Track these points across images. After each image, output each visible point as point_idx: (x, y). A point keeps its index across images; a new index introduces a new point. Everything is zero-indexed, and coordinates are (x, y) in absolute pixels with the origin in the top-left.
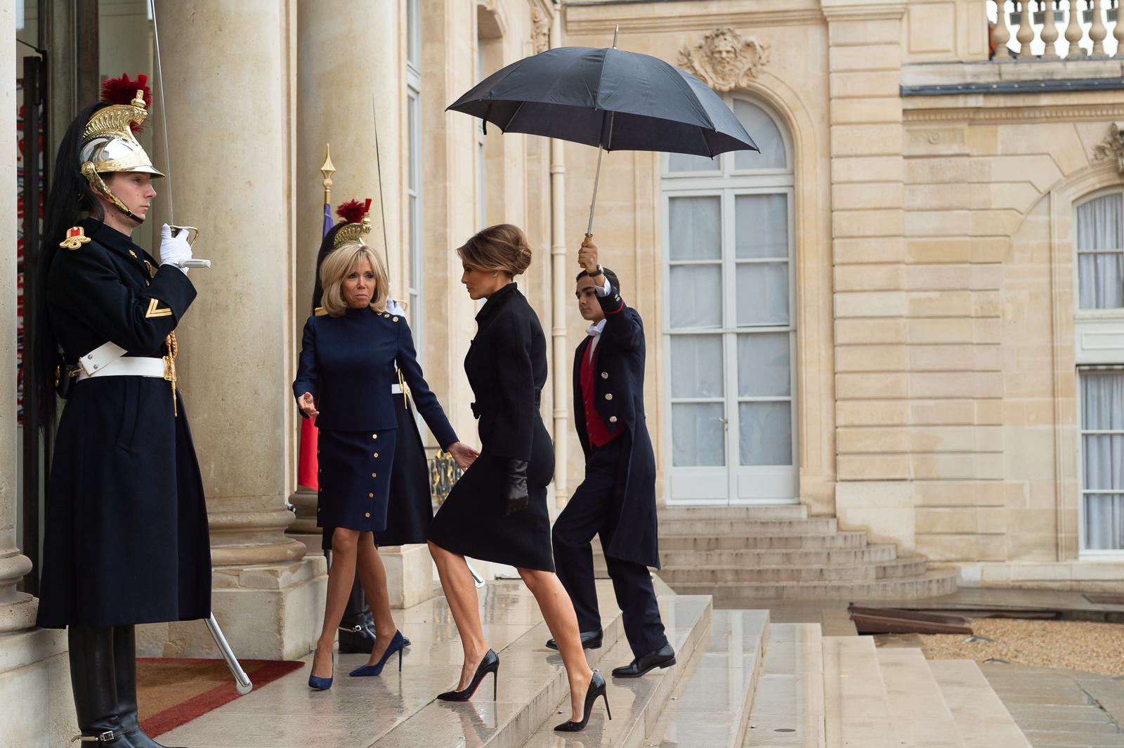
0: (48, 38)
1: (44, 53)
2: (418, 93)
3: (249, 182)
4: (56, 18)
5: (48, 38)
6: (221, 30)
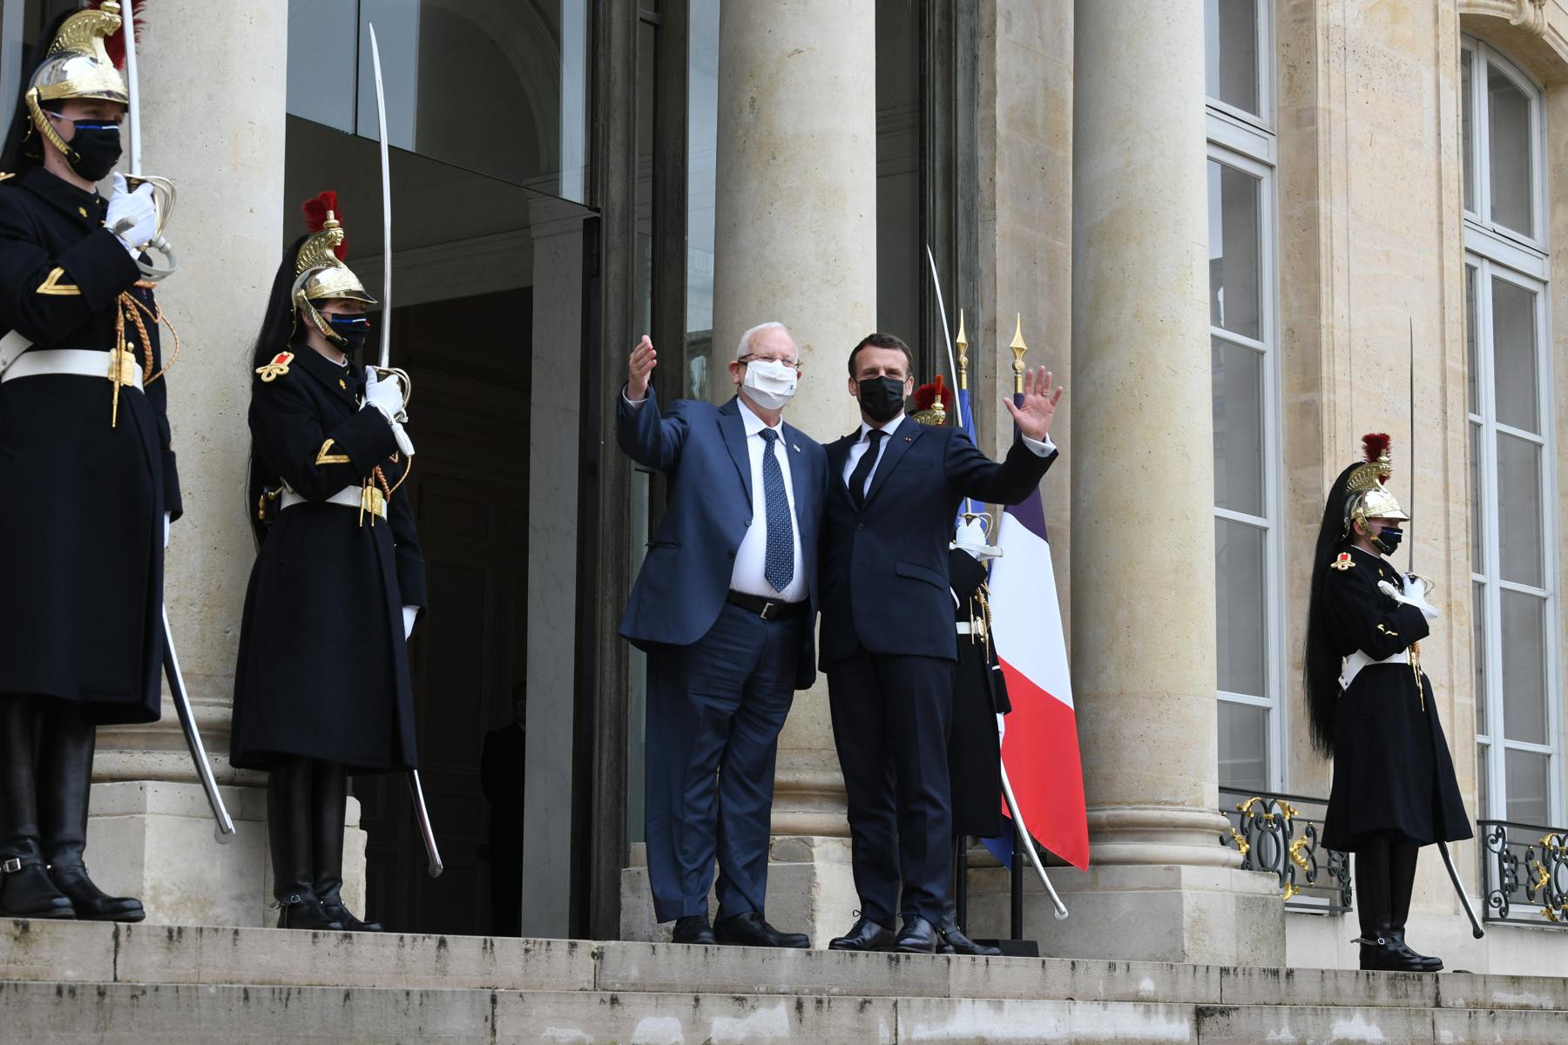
0: (602, 189)
1: (598, 210)
2: (1545, 283)
3: (808, 346)
4: (612, 167)
5: (602, 189)
6: (774, 158)
